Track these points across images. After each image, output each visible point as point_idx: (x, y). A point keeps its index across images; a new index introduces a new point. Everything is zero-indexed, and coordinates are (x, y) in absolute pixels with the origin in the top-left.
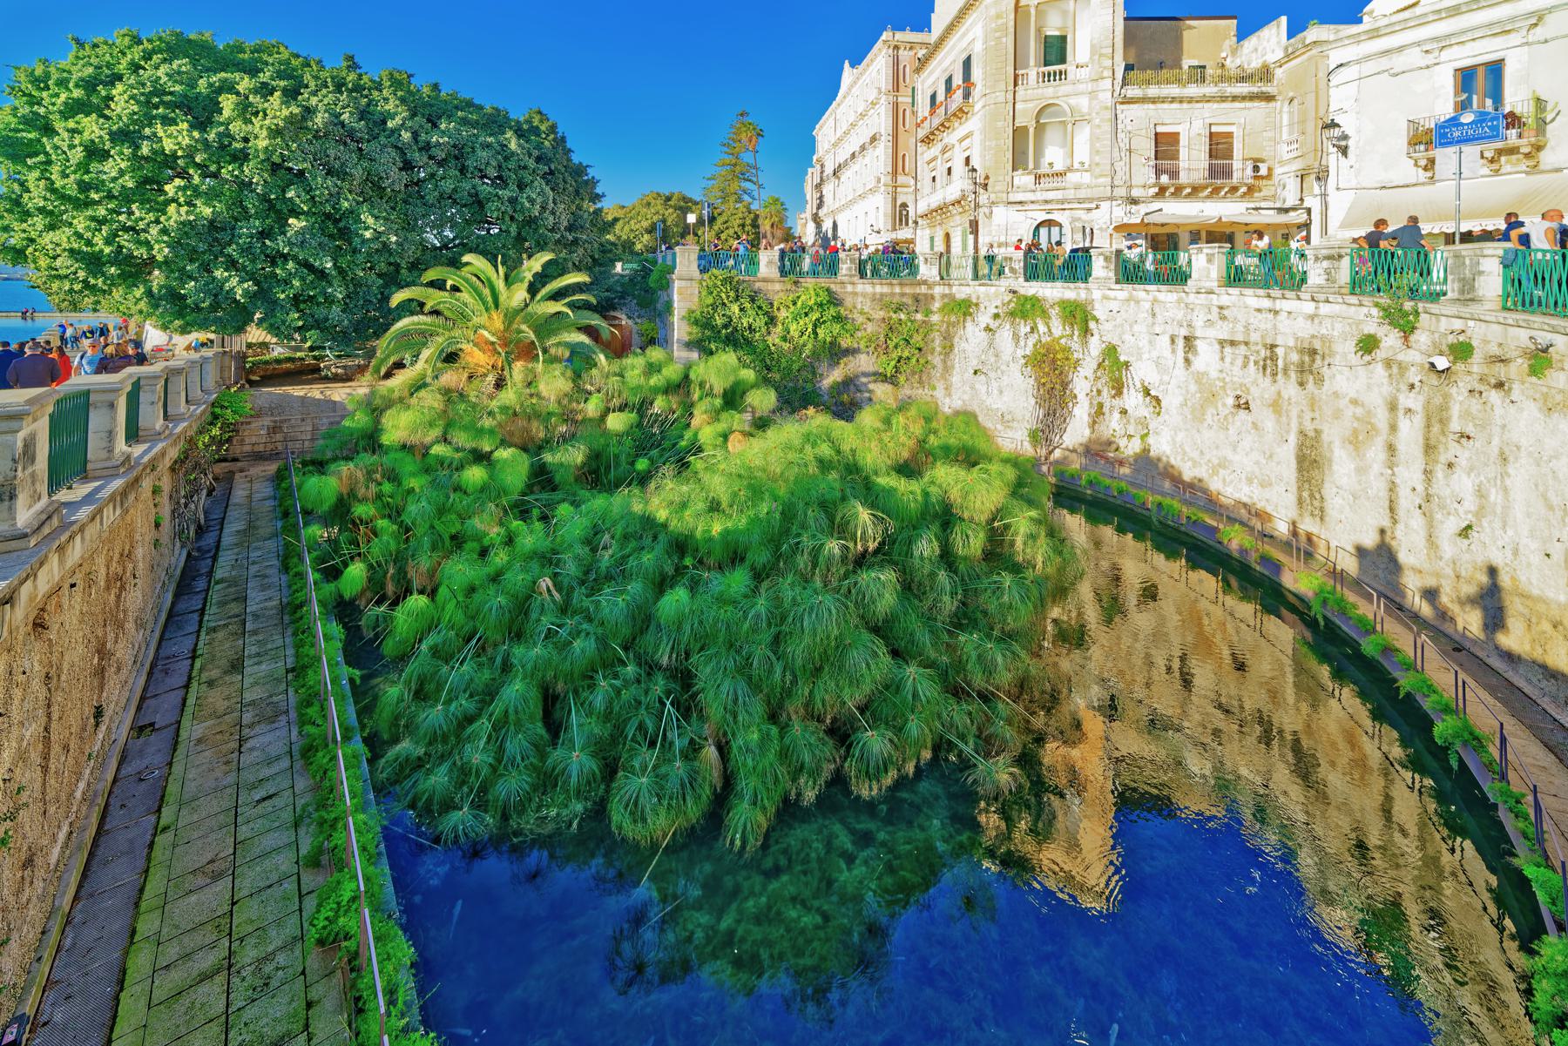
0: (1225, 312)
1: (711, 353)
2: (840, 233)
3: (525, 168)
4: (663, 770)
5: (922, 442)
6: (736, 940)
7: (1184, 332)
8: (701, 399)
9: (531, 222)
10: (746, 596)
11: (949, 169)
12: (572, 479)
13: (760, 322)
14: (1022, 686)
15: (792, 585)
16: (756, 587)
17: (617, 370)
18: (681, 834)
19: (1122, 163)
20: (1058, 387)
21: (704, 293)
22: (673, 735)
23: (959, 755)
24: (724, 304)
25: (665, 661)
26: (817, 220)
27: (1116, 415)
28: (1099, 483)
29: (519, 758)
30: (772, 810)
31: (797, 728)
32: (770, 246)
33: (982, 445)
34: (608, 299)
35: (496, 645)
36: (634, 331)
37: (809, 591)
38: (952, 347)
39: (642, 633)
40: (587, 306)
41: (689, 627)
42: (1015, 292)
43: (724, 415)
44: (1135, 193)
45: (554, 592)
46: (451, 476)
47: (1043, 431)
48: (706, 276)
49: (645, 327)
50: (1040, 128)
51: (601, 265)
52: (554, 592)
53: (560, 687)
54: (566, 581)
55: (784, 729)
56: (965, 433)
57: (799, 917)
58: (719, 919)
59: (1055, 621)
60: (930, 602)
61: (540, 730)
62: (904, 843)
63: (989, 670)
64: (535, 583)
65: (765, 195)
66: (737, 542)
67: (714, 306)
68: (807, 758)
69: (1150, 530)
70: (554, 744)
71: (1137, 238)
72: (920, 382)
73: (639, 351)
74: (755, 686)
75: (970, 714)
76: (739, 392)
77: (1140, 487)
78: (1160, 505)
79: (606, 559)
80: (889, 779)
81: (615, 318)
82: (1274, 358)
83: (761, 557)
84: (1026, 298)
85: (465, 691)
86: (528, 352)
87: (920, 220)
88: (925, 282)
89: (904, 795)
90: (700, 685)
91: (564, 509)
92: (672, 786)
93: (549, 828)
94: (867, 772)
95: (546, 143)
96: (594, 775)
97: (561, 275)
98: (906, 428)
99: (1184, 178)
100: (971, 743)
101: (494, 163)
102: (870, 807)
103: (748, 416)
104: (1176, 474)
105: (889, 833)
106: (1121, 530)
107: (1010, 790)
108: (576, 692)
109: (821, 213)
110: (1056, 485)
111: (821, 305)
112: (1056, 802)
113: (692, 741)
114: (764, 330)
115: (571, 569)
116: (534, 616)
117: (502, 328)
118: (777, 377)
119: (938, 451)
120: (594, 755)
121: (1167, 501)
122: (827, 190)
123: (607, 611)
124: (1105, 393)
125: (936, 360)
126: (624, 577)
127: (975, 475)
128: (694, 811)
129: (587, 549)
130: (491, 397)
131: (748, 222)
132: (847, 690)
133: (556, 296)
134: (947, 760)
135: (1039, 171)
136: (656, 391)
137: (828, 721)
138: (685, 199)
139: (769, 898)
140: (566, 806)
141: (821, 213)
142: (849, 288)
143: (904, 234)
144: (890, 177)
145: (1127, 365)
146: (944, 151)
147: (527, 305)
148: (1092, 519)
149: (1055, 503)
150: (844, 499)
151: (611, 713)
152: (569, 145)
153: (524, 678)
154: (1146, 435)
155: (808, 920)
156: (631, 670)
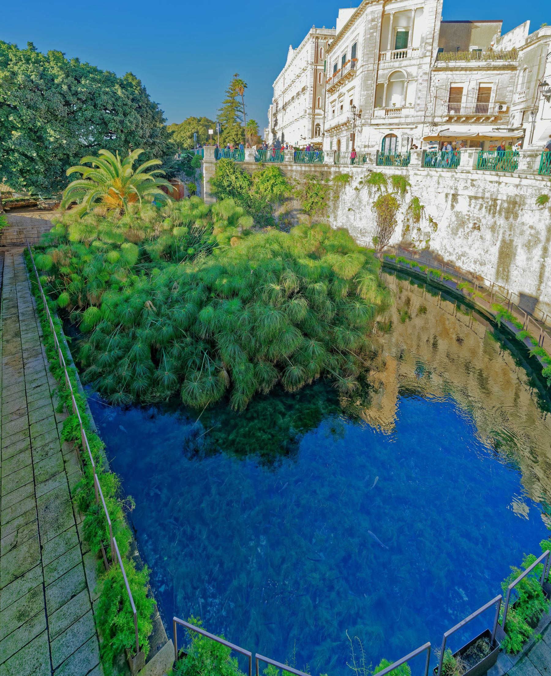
0: (474, 183)
1: (222, 199)
2: (285, 139)
3: (126, 105)
4: (204, 380)
5: (322, 243)
6: (236, 443)
7: (452, 192)
8: (217, 221)
9: (131, 133)
10: (239, 311)
11: (342, 106)
12: (158, 257)
13: (245, 184)
14: (361, 349)
15: (260, 306)
16: (243, 307)
17: (177, 207)
18: (212, 404)
19: (431, 104)
20: (388, 217)
21: (218, 170)
22: (208, 366)
23: (332, 375)
24: (228, 175)
25: (203, 336)
26: (274, 132)
27: (415, 231)
28: (404, 262)
29: (142, 374)
30: (250, 396)
31: (261, 364)
32: (250, 146)
33: (350, 245)
34: (171, 172)
35: (129, 328)
36: (185, 188)
37: (267, 309)
38: (338, 197)
39: (193, 325)
40: (162, 176)
41: (213, 322)
42: (371, 171)
43: (229, 229)
44: (437, 120)
45: (153, 307)
46: (103, 256)
47: (379, 238)
48: (219, 161)
49: (190, 186)
50: (390, 84)
51: (167, 155)
52: (153, 307)
53: (158, 346)
54: (158, 303)
55: (256, 365)
56: (342, 239)
57: (262, 436)
58: (229, 436)
59: (378, 322)
60: (322, 314)
61: (151, 363)
62: (307, 409)
63: (347, 342)
64: (144, 303)
65: (248, 119)
66: (234, 287)
67: (223, 177)
68: (266, 376)
69: (426, 283)
70: (157, 368)
71: (434, 144)
72: (322, 214)
73: (187, 198)
74: (243, 347)
75: (337, 360)
76: (235, 218)
77: (423, 264)
78: (432, 272)
79: (175, 293)
80: (301, 385)
81: (175, 181)
82: (495, 205)
83: (246, 294)
84: (376, 174)
85: (117, 347)
86: (134, 198)
87: (326, 133)
88: (327, 165)
89: (308, 392)
90: (219, 346)
91: (156, 271)
92: (208, 385)
93: (157, 400)
94: (292, 382)
95: (136, 92)
96: (174, 380)
97: (148, 160)
98: (314, 236)
99: (462, 112)
100: (337, 372)
101: (111, 102)
102: (293, 396)
103: (240, 229)
104: (441, 258)
105: (300, 405)
106: (412, 283)
107: (353, 390)
108: (165, 348)
109: (276, 129)
110: (384, 263)
111: (275, 176)
112: (372, 394)
113: (216, 369)
114: (247, 188)
115: (160, 297)
116: (145, 317)
117: (121, 186)
118: (254, 211)
119: (329, 247)
120: (174, 373)
121: (435, 271)
122: (279, 116)
123: (177, 315)
124: (411, 220)
125: (331, 204)
126: (184, 301)
127: (345, 259)
128: (217, 396)
129: (167, 289)
130: (119, 219)
131: (240, 133)
132: (283, 350)
133: (147, 171)
134: (326, 377)
135: (388, 108)
136: (196, 217)
137: (275, 362)
138: (207, 120)
139: (249, 428)
140: (163, 392)
141: (276, 129)
142: (289, 168)
143: (318, 140)
144: (311, 111)
145: (423, 207)
146: (339, 97)
147: (132, 176)
148: (399, 277)
149: (383, 270)
150: (284, 269)
151: (181, 356)
152: (148, 92)
153: (142, 342)
154: (429, 240)
155: (265, 437)
156: (188, 339)
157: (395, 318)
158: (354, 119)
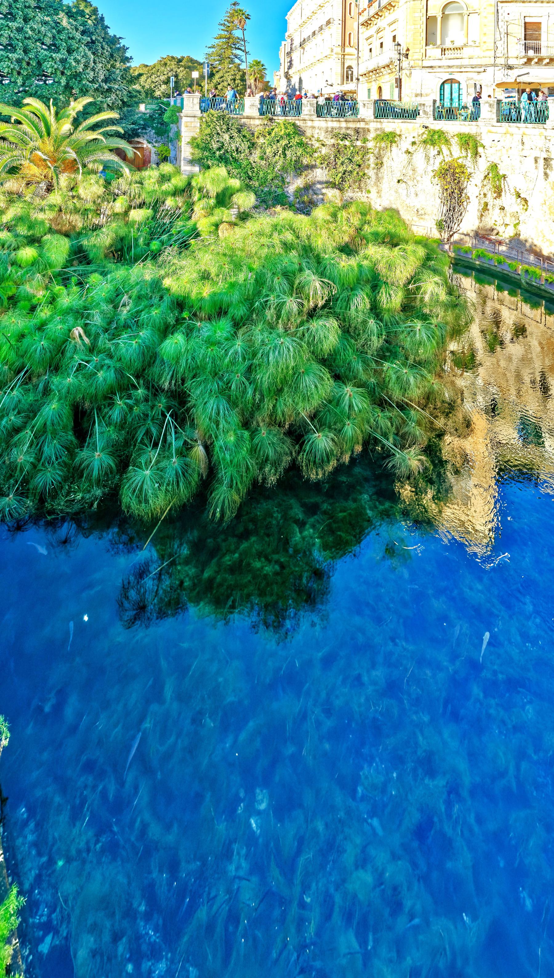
1: (209, 167)
2: (304, 85)
3: (73, 38)
4: (162, 464)
5: (359, 230)
6: (215, 585)
8: (200, 199)
9: (77, 76)
10: (227, 339)
11: (382, 44)
13: (244, 146)
14: (428, 398)
15: (262, 331)
16: (235, 333)
17: (138, 179)
18: (176, 511)
19: (502, 42)
20: (456, 191)
21: (204, 126)
22: (172, 438)
23: (383, 447)
24: (218, 134)
25: (166, 386)
26: (287, 76)
27: (497, 210)
28: (485, 256)
29: (54, 458)
30: (243, 491)
31: (263, 431)
32: (252, 94)
33: (401, 232)
34: (133, 130)
36: (153, 152)
37: (274, 335)
38: (382, 163)
39: (149, 366)
40: (118, 135)
41: (184, 361)
42: (426, 127)
43: (217, 211)
44: (511, 62)
45: (85, 338)
47: (446, 221)
48: (205, 115)
49: (160, 149)
50: (445, 17)
51: (129, 106)
52: (85, 338)
54: (93, 330)
55: (254, 433)
56: (389, 223)
57: (262, 568)
58: (202, 571)
59: (452, 352)
60: (362, 341)
61: (71, 436)
62: (341, 511)
63: (404, 389)
64: (70, 331)
65: (251, 59)
66: (221, 302)
67: (211, 136)
68: (271, 453)
69: (520, 288)
70: (81, 447)
71: (512, 92)
72: (360, 188)
73: (154, 166)
74: (233, 403)
75: (390, 419)
76: (228, 195)
77: (512, 259)
78: (527, 271)
79: (124, 313)
80: (330, 467)
81: (139, 143)
83: (240, 311)
84: (435, 132)
85: (14, 410)
87: (360, 78)
88: (363, 120)
89: (344, 479)
90: (193, 402)
92: (170, 475)
94: (315, 462)
95: (90, 22)
96: (111, 468)
97: (98, 113)
98: (348, 220)
100: (391, 439)
101: (50, 35)
102: (317, 485)
103: (234, 211)
104: (538, 250)
105: (331, 504)
106: (500, 289)
107: (419, 472)
108: (99, 409)
109: (291, 72)
110: (455, 259)
111: (289, 135)
112: (450, 477)
113: (185, 443)
114: (247, 151)
115: (97, 320)
116: (68, 355)
117: (52, 149)
118: (257, 184)
119: (370, 236)
120: (112, 454)
121: (532, 269)
122: (295, 56)
123: (124, 350)
124: (489, 195)
125: (371, 172)
126: (138, 326)
127: (396, 253)
128: (184, 492)
129: (111, 306)
131: (238, 77)
132: (300, 404)
133: (94, 127)
134: (374, 450)
135: (444, 47)
136: (166, 194)
137: (287, 426)
138: (191, 60)
139: (240, 554)
140: (89, 492)
141: (291, 72)
142: (309, 124)
143: (350, 86)
144: (340, 48)
145: (504, 177)
146: (378, 32)
147: (71, 134)
148: (479, 280)
149: (454, 270)
150: (301, 270)
151: (125, 423)
152: (106, 23)
153: (60, 399)
154: (518, 224)
155: (268, 569)
156: (141, 392)
157: (480, 344)
158: (400, 60)
